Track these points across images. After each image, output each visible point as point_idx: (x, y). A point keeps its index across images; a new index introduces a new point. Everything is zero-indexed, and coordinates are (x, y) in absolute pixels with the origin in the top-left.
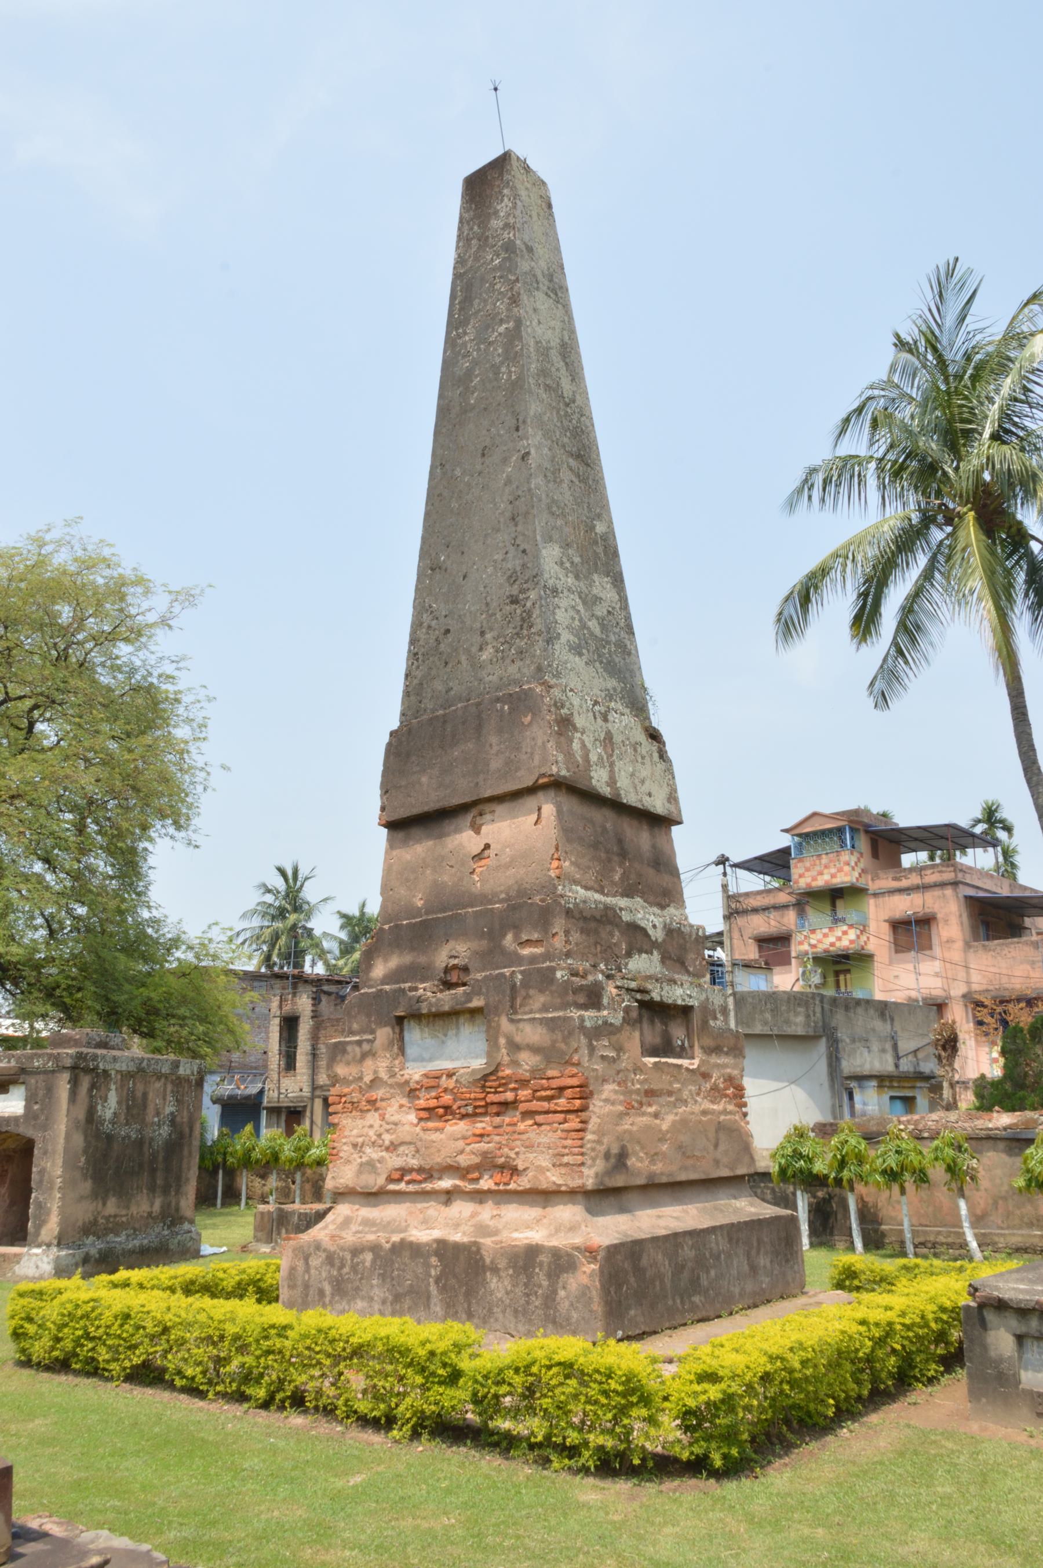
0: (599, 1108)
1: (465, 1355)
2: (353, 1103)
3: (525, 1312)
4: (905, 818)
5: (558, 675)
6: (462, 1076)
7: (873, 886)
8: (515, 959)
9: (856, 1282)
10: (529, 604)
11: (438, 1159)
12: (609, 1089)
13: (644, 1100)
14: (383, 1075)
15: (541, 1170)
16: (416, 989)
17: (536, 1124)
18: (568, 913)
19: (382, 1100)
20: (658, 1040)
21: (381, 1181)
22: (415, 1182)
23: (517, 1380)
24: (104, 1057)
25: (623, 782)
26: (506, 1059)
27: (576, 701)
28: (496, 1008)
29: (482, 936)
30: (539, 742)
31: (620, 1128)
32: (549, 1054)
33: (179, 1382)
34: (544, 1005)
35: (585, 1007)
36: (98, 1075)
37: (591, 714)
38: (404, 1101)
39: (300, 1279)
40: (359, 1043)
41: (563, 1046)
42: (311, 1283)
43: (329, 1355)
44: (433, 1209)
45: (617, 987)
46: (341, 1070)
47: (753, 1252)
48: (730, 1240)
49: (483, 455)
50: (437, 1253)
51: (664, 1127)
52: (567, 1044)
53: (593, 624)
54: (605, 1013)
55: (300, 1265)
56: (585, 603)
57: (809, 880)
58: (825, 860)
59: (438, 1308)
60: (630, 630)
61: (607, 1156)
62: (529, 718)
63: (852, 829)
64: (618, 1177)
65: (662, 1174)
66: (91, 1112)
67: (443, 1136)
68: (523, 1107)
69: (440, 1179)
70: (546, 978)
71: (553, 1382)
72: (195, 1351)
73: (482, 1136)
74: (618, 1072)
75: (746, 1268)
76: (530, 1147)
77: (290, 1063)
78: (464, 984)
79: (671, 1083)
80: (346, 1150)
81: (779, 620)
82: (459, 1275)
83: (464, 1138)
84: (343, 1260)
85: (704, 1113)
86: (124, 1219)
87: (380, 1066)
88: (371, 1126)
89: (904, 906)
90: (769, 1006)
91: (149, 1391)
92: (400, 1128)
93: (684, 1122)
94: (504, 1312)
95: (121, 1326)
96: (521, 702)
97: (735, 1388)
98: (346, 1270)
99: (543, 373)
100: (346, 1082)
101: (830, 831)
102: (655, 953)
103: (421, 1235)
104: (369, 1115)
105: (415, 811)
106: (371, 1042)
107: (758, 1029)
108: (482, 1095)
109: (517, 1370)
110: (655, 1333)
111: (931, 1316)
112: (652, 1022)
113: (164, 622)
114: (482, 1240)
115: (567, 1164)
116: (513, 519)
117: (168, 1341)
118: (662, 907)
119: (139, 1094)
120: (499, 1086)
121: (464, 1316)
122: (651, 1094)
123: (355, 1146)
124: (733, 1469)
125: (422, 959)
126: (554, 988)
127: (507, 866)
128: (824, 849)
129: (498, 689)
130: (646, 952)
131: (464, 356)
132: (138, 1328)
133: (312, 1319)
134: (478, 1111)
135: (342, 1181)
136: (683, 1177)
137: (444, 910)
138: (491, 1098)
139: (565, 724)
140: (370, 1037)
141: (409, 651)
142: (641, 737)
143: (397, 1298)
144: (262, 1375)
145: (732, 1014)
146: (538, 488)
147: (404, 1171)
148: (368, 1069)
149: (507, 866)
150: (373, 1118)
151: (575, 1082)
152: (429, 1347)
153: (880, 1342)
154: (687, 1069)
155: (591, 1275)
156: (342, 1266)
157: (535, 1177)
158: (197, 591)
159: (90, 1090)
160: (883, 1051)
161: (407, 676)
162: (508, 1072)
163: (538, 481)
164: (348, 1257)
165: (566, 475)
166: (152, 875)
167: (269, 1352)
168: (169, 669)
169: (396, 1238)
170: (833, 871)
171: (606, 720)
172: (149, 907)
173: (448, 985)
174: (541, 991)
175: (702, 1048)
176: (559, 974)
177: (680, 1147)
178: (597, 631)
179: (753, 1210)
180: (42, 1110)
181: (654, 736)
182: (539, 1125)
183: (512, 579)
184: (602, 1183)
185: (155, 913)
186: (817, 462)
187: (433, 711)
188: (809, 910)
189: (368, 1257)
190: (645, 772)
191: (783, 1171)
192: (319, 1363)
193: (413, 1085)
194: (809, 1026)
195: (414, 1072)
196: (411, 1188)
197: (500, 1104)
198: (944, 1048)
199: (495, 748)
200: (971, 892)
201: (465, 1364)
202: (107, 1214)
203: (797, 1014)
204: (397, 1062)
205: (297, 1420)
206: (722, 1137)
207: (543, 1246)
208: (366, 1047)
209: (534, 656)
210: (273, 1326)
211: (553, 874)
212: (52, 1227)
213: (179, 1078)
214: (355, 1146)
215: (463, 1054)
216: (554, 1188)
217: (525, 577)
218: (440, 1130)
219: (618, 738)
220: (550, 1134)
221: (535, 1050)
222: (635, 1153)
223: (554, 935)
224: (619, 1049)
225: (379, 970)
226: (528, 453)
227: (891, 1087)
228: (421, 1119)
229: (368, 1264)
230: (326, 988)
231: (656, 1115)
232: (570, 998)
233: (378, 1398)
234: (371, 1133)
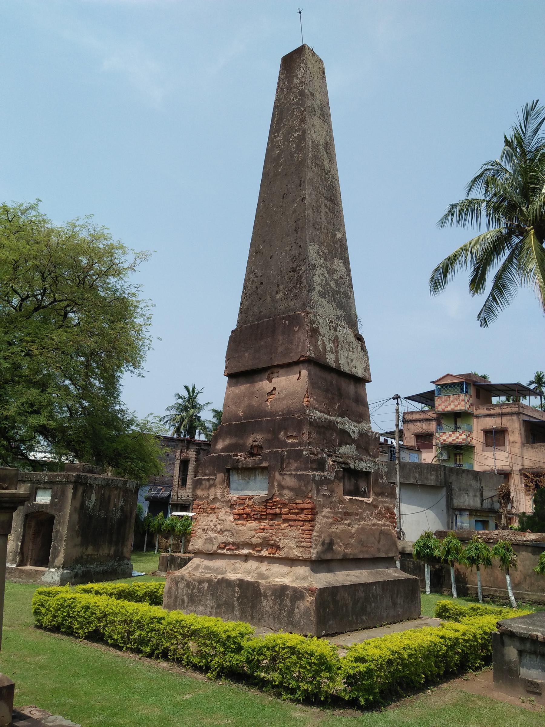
0: (320, 520)
1: (245, 639)
2: (204, 509)
3: (278, 619)
4: (494, 379)
5: (313, 308)
6: (256, 499)
7: (476, 412)
8: (285, 445)
9: (448, 614)
10: (301, 272)
12: (326, 510)
14: (219, 496)
15: (291, 548)
16: (237, 456)
17: (289, 525)
18: (311, 423)
19: (218, 508)
20: (352, 488)
21: (215, 548)
22: (231, 550)
23: (268, 653)
24: (90, 477)
25: (342, 361)
26: (277, 492)
27: (321, 321)
30: (302, 340)
31: (330, 530)
32: (298, 492)
33: (110, 641)
34: (296, 468)
35: (316, 470)
37: (328, 327)
38: (228, 510)
39: (173, 593)
40: (208, 480)
41: (304, 489)
42: (179, 596)
43: (181, 634)
44: (239, 563)
45: (333, 461)
46: (199, 493)
47: (395, 596)
48: (383, 589)
49: (283, 197)
51: (353, 531)
52: (306, 488)
53: (332, 283)
54: (326, 473)
56: (329, 273)
57: (444, 407)
58: (452, 398)
59: (237, 613)
60: (351, 286)
61: (323, 544)
63: (467, 384)
65: (350, 554)
66: (83, 504)
67: (245, 528)
68: (284, 517)
69: (242, 549)
70: (297, 455)
71: (285, 656)
72: (119, 627)
73: (264, 529)
74: (331, 503)
76: (286, 537)
77: (183, 483)
78: (260, 455)
79: (357, 509)
80: (199, 532)
81: (432, 281)
83: (255, 530)
84: (194, 585)
85: (374, 525)
86: (96, 557)
87: (217, 492)
88: (212, 521)
89: (491, 423)
90: (417, 470)
91: (96, 645)
92: (225, 523)
93: (363, 529)
94: (268, 617)
95: (85, 612)
96: (294, 320)
97: (373, 666)
98: (195, 591)
99: (315, 157)
100: (201, 498)
101: (456, 383)
102: (353, 445)
103: (232, 576)
104: (211, 515)
106: (214, 480)
107: (412, 481)
108: (265, 510)
109: (268, 649)
110: (342, 633)
111: (479, 636)
112: (350, 479)
113: (132, 268)
114: (260, 581)
115: (303, 546)
116: (296, 230)
117: (106, 621)
118: (359, 422)
119: (106, 496)
120: (273, 505)
121: (250, 618)
122: (347, 514)
123: (203, 530)
124: (370, 707)
125: (241, 442)
126: (302, 460)
127: (283, 399)
128: (452, 392)
129: (284, 313)
131: (277, 148)
132: (93, 613)
133: (174, 615)
134: (263, 517)
135: (196, 547)
136: (361, 556)
137: (252, 418)
138: (269, 511)
139: (315, 332)
140: (214, 477)
141: (243, 292)
142: (352, 338)
143: (219, 606)
144: (149, 641)
145: (398, 473)
146: (308, 215)
147: (226, 544)
149: (283, 399)
150: (213, 517)
151: (309, 506)
152: (227, 633)
153: (451, 648)
155: (311, 603)
156: (194, 589)
157: (288, 551)
158: (149, 253)
159: (83, 493)
160: (475, 496)
161: (241, 304)
162: (278, 499)
163: (309, 212)
165: (323, 209)
166: (122, 389)
167: (153, 630)
168: (134, 290)
169: (220, 577)
170: (456, 403)
171: (335, 330)
172: (120, 404)
173: (252, 455)
174: (296, 461)
175: (374, 493)
176: (304, 453)
177: (361, 541)
178: (334, 286)
179: (396, 574)
180: (59, 502)
181: (360, 338)
182: (291, 526)
183: (293, 260)
184: (320, 557)
185: (122, 407)
186: (456, 201)
187: (253, 321)
188: (443, 421)
189: (206, 585)
190: (353, 356)
191: (418, 553)
192: (176, 637)
193: (232, 502)
194: (438, 481)
195: (234, 496)
196: (229, 552)
197: (273, 514)
198: (503, 499)
199: (281, 342)
200: (526, 418)
201: (244, 644)
202: (88, 554)
203: (431, 475)
204: (226, 490)
205: (164, 665)
206: (382, 537)
207: (289, 586)
208: (211, 482)
209: (302, 298)
210: (155, 618)
211: (304, 404)
212: (60, 559)
213: (126, 489)
214: (203, 530)
215: (257, 490)
216: (297, 558)
217: (299, 259)
218: (245, 525)
219: (341, 339)
221: (291, 489)
222: (338, 543)
223: (303, 434)
224: (332, 491)
225: (220, 445)
226: (305, 198)
227: (476, 515)
230: (203, 447)
231: (349, 525)
232: (309, 465)
233: (203, 657)
234: (212, 524)
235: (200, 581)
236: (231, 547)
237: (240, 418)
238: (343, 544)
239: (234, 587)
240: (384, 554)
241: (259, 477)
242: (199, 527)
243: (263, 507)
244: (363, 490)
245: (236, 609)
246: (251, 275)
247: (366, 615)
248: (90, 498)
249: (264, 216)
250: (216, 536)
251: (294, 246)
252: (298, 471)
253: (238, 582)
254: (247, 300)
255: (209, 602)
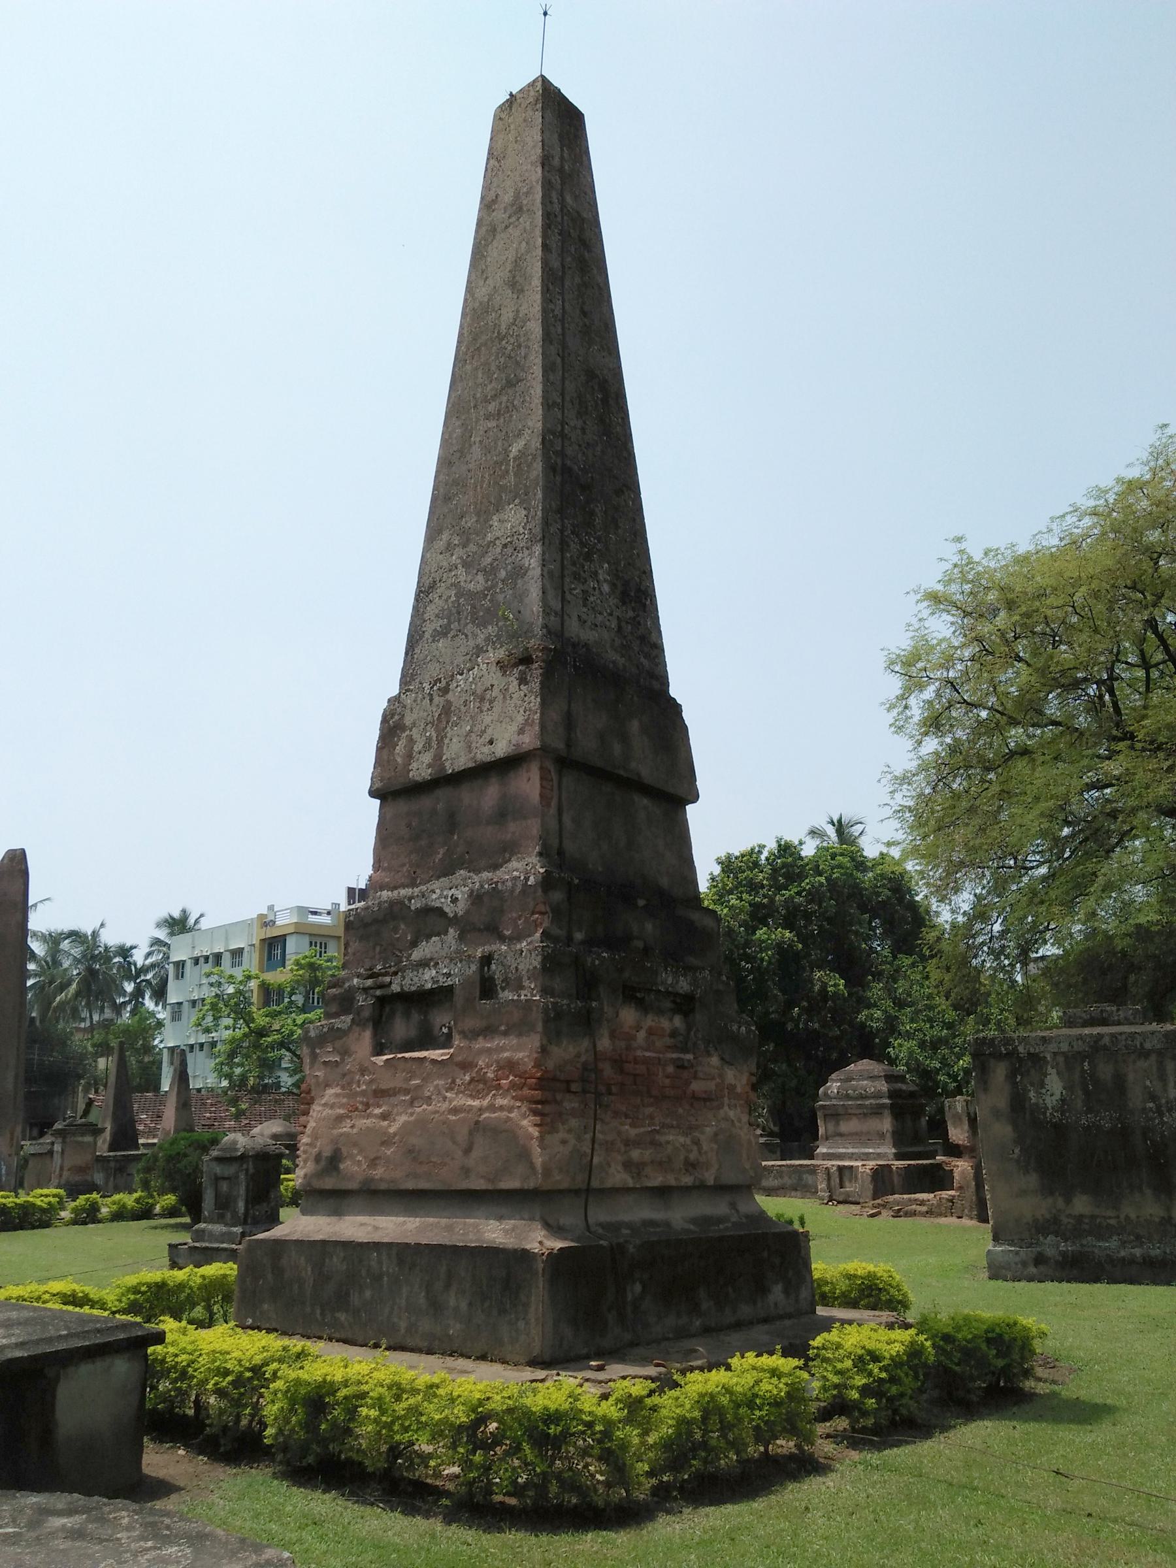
13: (371, 1102)
31: (335, 1132)
36: (1020, 1060)
61: (318, 1159)
64: (327, 1180)
65: (381, 1179)
74: (344, 1075)
75: (422, 1300)
85: (455, 1111)
86: (1113, 1222)
93: (422, 1124)
102: (451, 931)
112: (407, 1015)
130: (438, 934)
136: (410, 1185)
154: (434, 1061)
177: (410, 1152)
184: (309, 1184)
224: (345, 1052)
231: (384, 1117)
238: (365, 1157)
240: (482, 1181)
244: (445, 1030)
247: (347, 1312)
248: (1042, 1084)
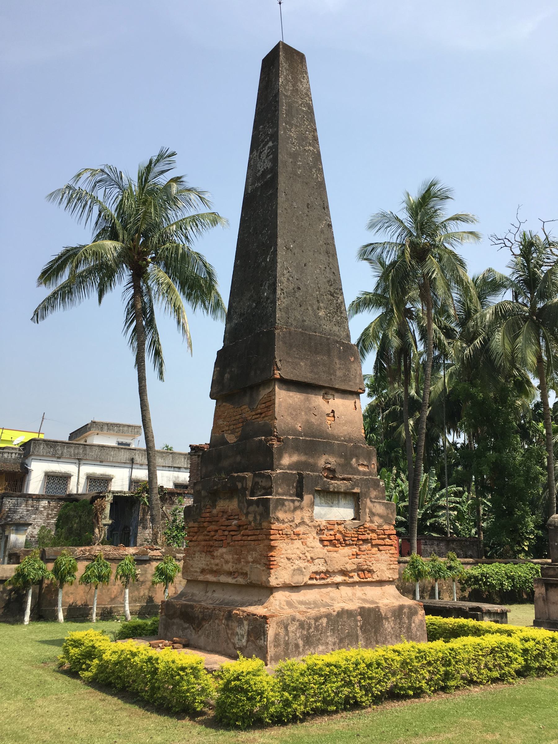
2: (287, 535)
11: (337, 567)
14: (307, 521)
15: (383, 571)
17: (379, 550)
26: (368, 519)
28: (365, 494)
29: (341, 456)
38: (315, 535)
40: (293, 501)
41: (391, 516)
50: (360, 614)
55: (282, 632)
62: (352, 359)
67: (338, 555)
68: (374, 542)
82: (370, 623)
87: (306, 515)
92: (315, 550)
98: (311, 630)
100: (283, 522)
103: (352, 606)
104: (295, 541)
105: (300, 379)
108: (357, 536)
123: (289, 559)
125: (311, 460)
127: (344, 425)
135: (281, 580)
138: (361, 537)
143: (341, 640)
147: (316, 573)
148: (298, 516)
149: (344, 425)
156: (310, 628)
162: (368, 525)
164: (313, 622)
189: (324, 621)
193: (322, 528)
199: (338, 366)
205: (475, 691)
214: (289, 559)
216: (388, 579)
220: (386, 555)
221: (381, 516)
228: (324, 546)
229: (324, 625)
234: (298, 552)
235: (317, 617)
236: (322, 575)
237: (300, 434)
239: (355, 617)
241: (342, 502)
242: (282, 556)
243: (355, 533)
245: (360, 638)
246: (285, 271)
249: (289, 211)
250: (307, 566)
251: (328, 269)
252: (377, 499)
253: (359, 610)
254: (284, 298)
255: (330, 639)
